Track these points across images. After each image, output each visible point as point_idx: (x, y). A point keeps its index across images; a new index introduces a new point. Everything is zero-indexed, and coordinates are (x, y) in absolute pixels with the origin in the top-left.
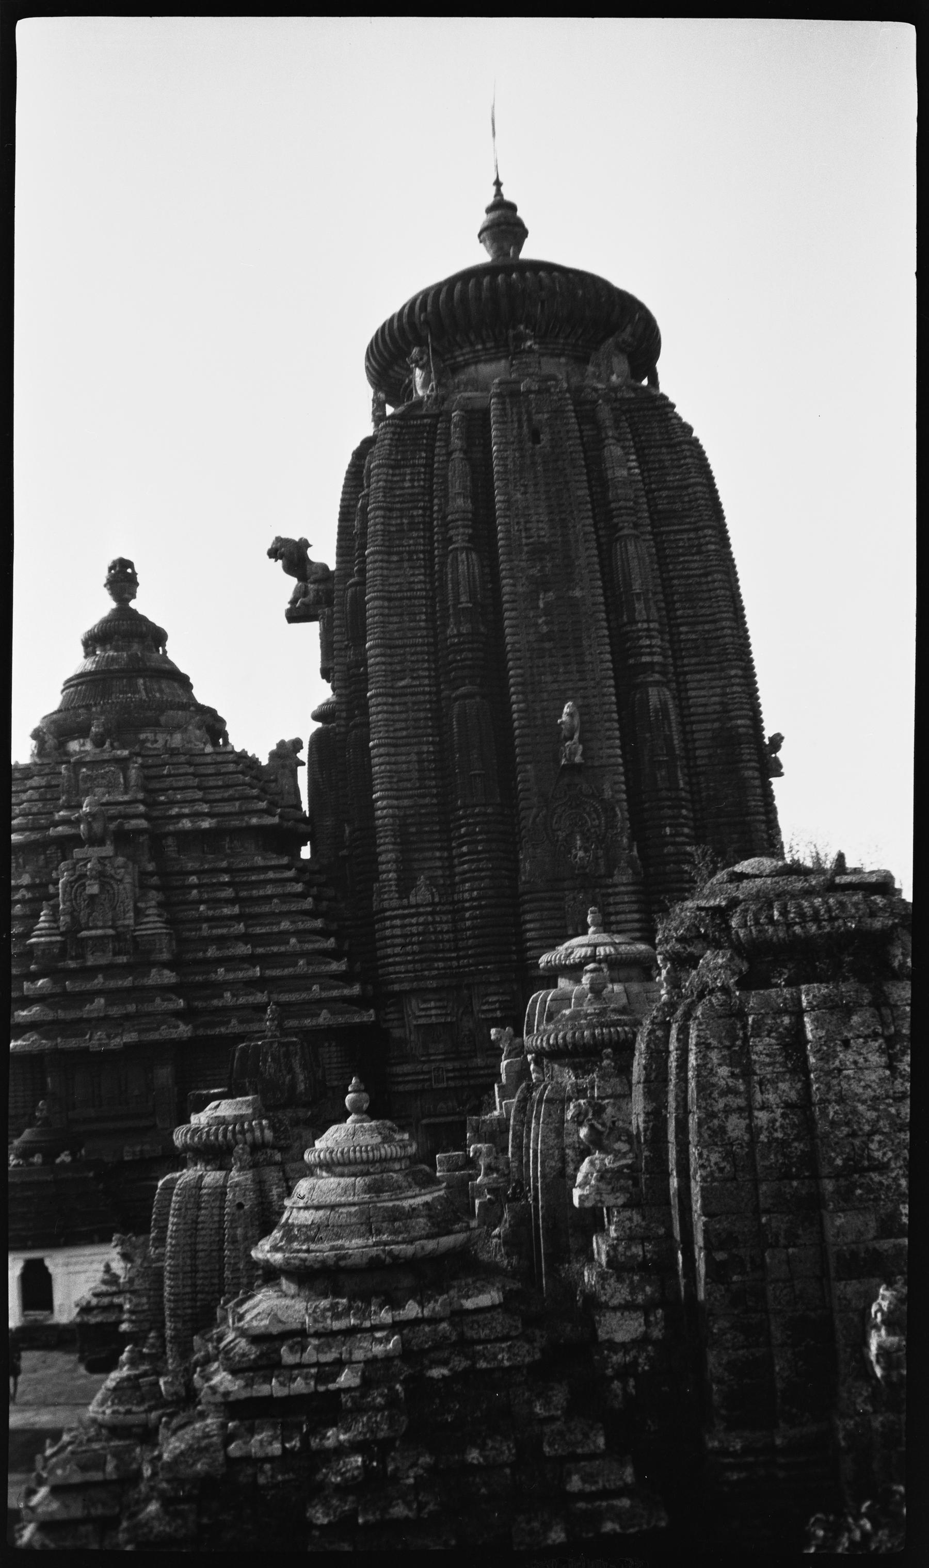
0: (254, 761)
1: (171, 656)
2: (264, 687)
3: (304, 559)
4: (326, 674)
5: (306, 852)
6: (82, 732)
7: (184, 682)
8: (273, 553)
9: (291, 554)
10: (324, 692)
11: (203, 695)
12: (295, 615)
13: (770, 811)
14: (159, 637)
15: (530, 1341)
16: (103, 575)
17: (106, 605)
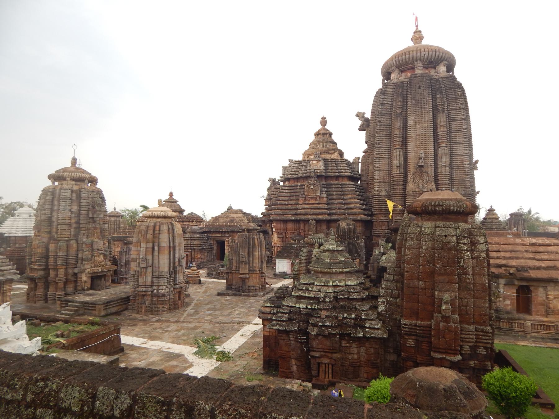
0: (349, 162)
1: (333, 138)
2: (353, 145)
3: (363, 117)
4: (366, 143)
5: (359, 182)
6: (312, 154)
7: (335, 144)
8: (357, 115)
9: (360, 115)
10: (366, 146)
11: (339, 147)
12: (360, 130)
13: (472, 178)
14: (331, 134)
15: (364, 293)
16: (319, 120)
17: (319, 127)
